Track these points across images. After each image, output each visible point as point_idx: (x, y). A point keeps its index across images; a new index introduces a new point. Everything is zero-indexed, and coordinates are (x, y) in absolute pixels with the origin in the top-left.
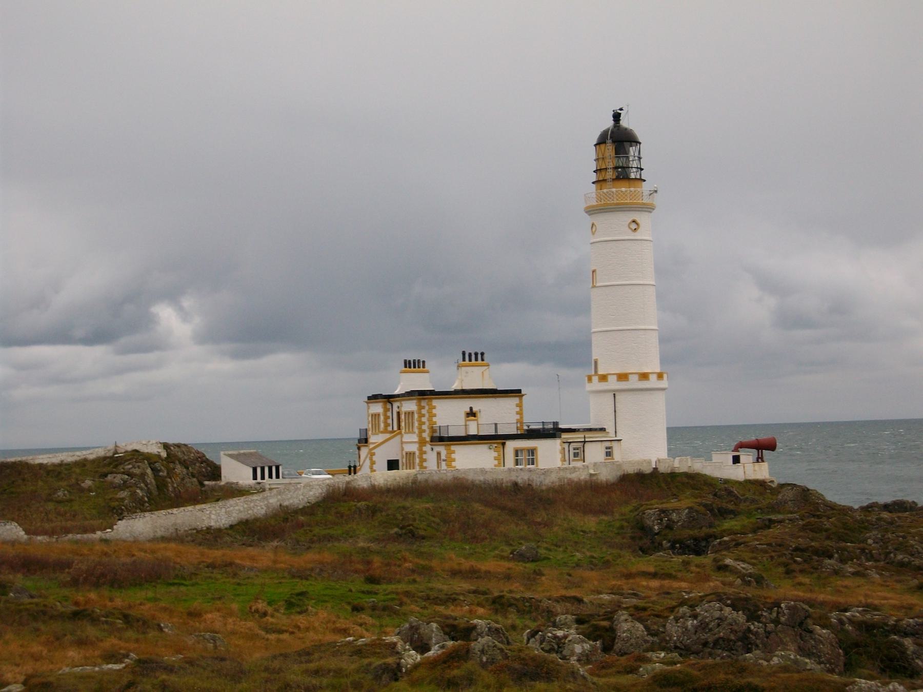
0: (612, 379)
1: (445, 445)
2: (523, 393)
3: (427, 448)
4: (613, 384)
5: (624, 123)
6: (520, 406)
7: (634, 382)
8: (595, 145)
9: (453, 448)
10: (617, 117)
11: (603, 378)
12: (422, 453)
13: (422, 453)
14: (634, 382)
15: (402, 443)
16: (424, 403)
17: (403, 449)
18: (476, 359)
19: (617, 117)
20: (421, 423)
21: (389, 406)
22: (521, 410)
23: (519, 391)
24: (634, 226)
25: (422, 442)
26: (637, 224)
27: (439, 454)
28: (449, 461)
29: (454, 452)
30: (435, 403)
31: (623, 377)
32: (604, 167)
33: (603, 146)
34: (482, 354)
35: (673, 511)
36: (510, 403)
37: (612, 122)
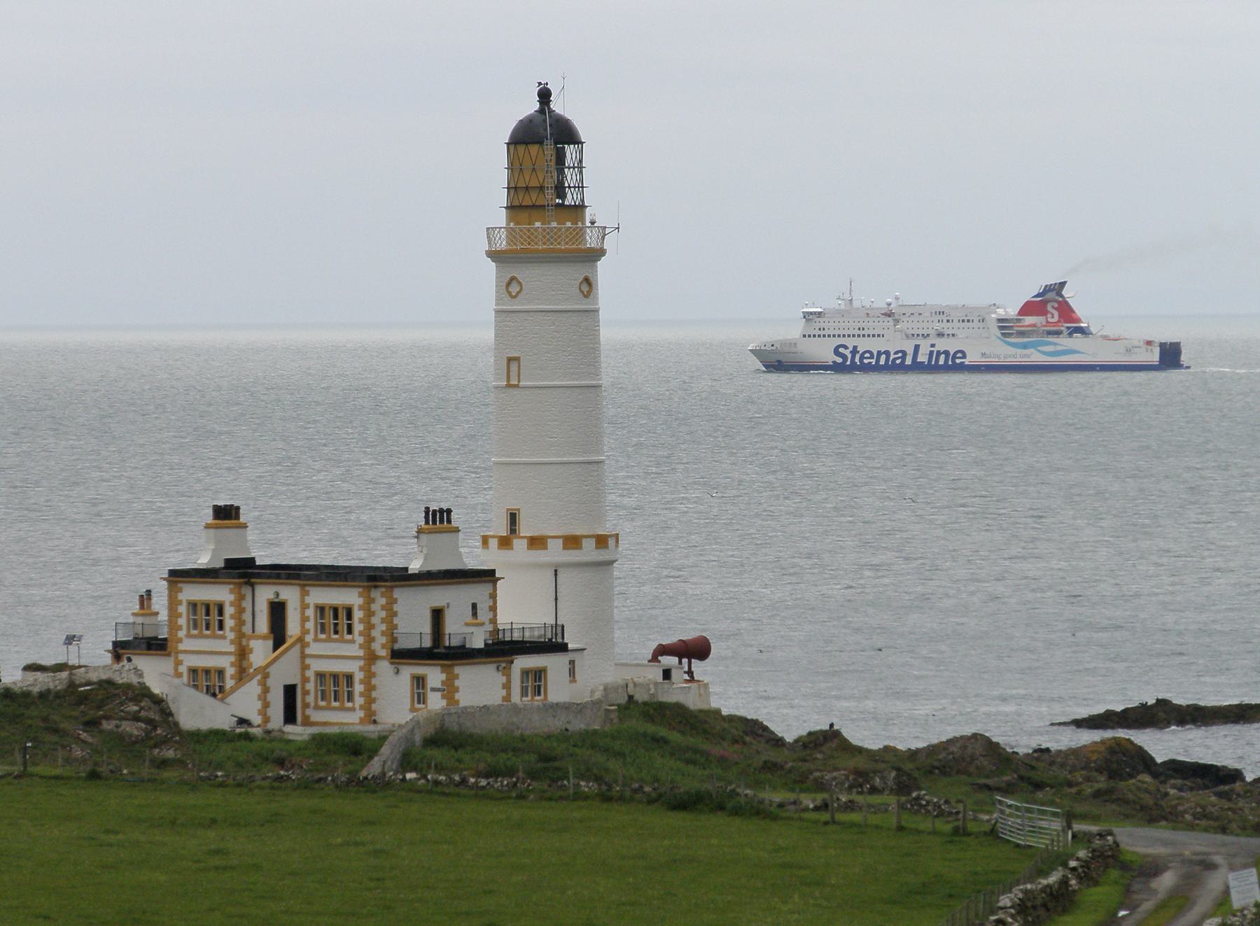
0: (555, 546)
1: (442, 666)
2: (497, 575)
3: (384, 668)
4: (555, 552)
5: (557, 106)
6: (493, 596)
7: (589, 552)
8: (508, 144)
9: (457, 670)
10: (545, 95)
11: (537, 542)
12: (369, 675)
13: (369, 675)
14: (589, 552)
15: (303, 656)
16: (376, 594)
17: (305, 667)
18: (442, 521)
19: (545, 95)
20: (370, 627)
21: (247, 591)
22: (495, 603)
23: (491, 573)
24: (585, 288)
25: (371, 658)
26: (590, 284)
27: (419, 681)
28: (449, 690)
29: (457, 677)
30: (398, 593)
31: (572, 542)
32: (534, 183)
33: (521, 148)
34: (449, 511)
35: (875, 772)
36: (477, 593)
37: (537, 106)
